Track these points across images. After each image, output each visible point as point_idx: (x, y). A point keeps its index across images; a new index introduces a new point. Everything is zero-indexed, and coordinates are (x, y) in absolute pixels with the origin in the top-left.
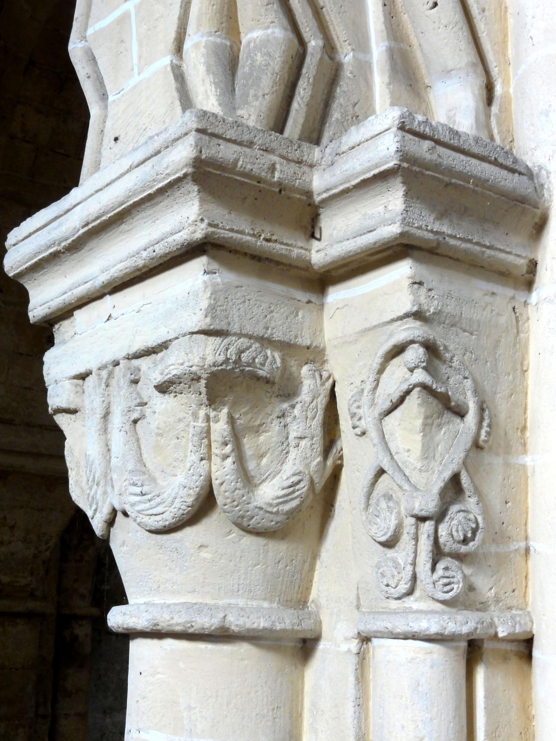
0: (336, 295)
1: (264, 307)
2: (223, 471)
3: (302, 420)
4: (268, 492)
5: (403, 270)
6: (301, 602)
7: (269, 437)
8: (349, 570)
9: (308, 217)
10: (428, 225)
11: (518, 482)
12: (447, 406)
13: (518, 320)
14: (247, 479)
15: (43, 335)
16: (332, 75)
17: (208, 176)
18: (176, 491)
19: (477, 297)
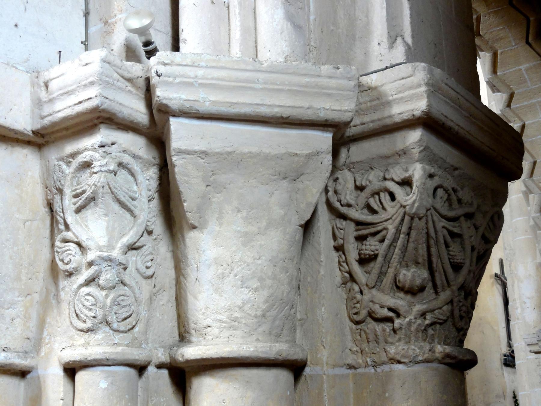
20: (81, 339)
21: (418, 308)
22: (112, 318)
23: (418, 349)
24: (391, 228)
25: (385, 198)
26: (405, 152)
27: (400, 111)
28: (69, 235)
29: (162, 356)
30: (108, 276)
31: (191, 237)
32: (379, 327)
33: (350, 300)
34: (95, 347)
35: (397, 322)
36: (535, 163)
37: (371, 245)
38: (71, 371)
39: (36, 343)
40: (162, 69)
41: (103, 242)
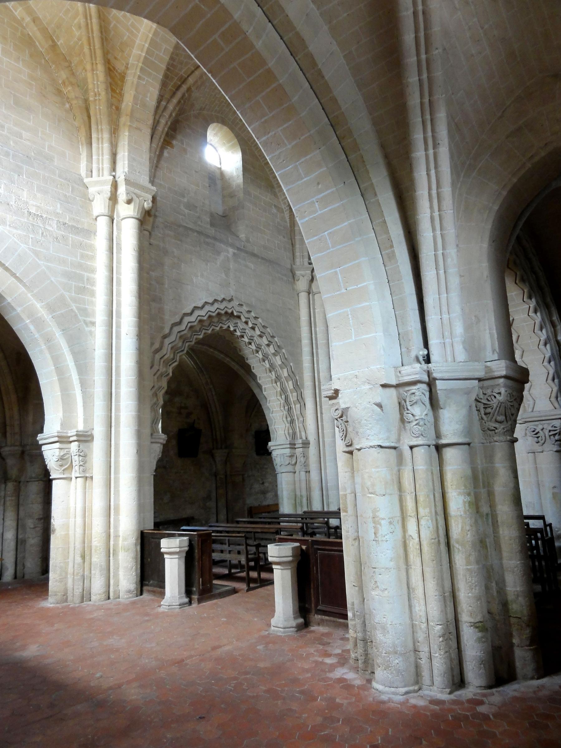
1: (293, 451)
3: (295, 457)
6: (294, 469)
8: (298, 468)
9: (295, 445)
10: (303, 446)
11: (309, 462)
17: (290, 444)
18: (287, 463)
19: (306, 449)
20: (415, 439)
21: (502, 427)
22: (423, 434)
23: (502, 438)
24: (495, 406)
25: (493, 397)
26: (498, 385)
27: (497, 374)
28: (409, 412)
29: (434, 443)
30: (421, 423)
31: (441, 411)
32: (490, 432)
33: (481, 425)
34: (420, 441)
35: (496, 431)
36: (519, 336)
37: (489, 410)
38: (411, 448)
39: (399, 440)
40: (434, 368)
41: (419, 414)
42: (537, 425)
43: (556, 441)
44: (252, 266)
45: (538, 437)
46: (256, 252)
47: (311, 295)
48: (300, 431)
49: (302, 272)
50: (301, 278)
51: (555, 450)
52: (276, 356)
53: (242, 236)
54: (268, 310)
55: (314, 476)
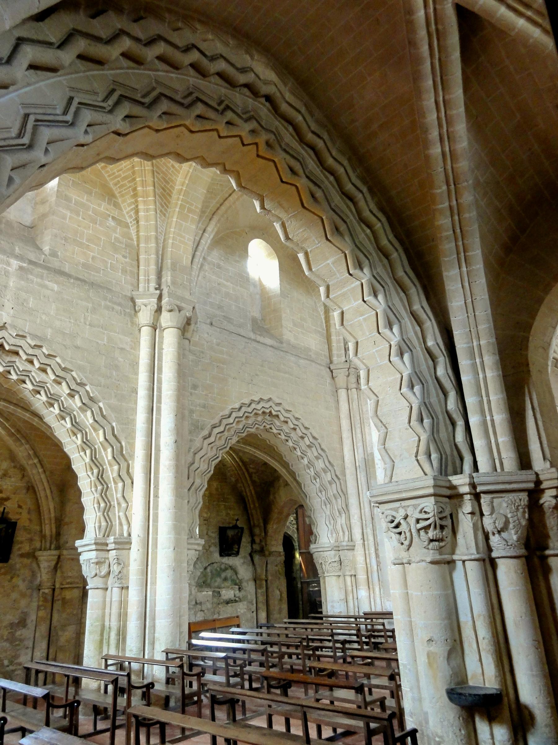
0: (110, 552)
1: (103, 554)
2: (98, 571)
4: (103, 573)
5: (115, 551)
6: (106, 584)
7: (103, 567)
9: (107, 545)
10: (117, 547)
11: (128, 571)
12: (120, 564)
13: (129, 553)
14: (100, 572)
15: (80, 554)
16: (112, 526)
17: (96, 544)
18: (93, 574)
36: (357, 343)
42: (396, 510)
43: (432, 541)
44: (56, 287)
45: (400, 533)
46: (67, 270)
47: (157, 331)
48: (121, 524)
49: (145, 301)
50: (143, 307)
51: (429, 559)
52: (86, 411)
53: (46, 249)
54: (77, 347)
55: (134, 596)
